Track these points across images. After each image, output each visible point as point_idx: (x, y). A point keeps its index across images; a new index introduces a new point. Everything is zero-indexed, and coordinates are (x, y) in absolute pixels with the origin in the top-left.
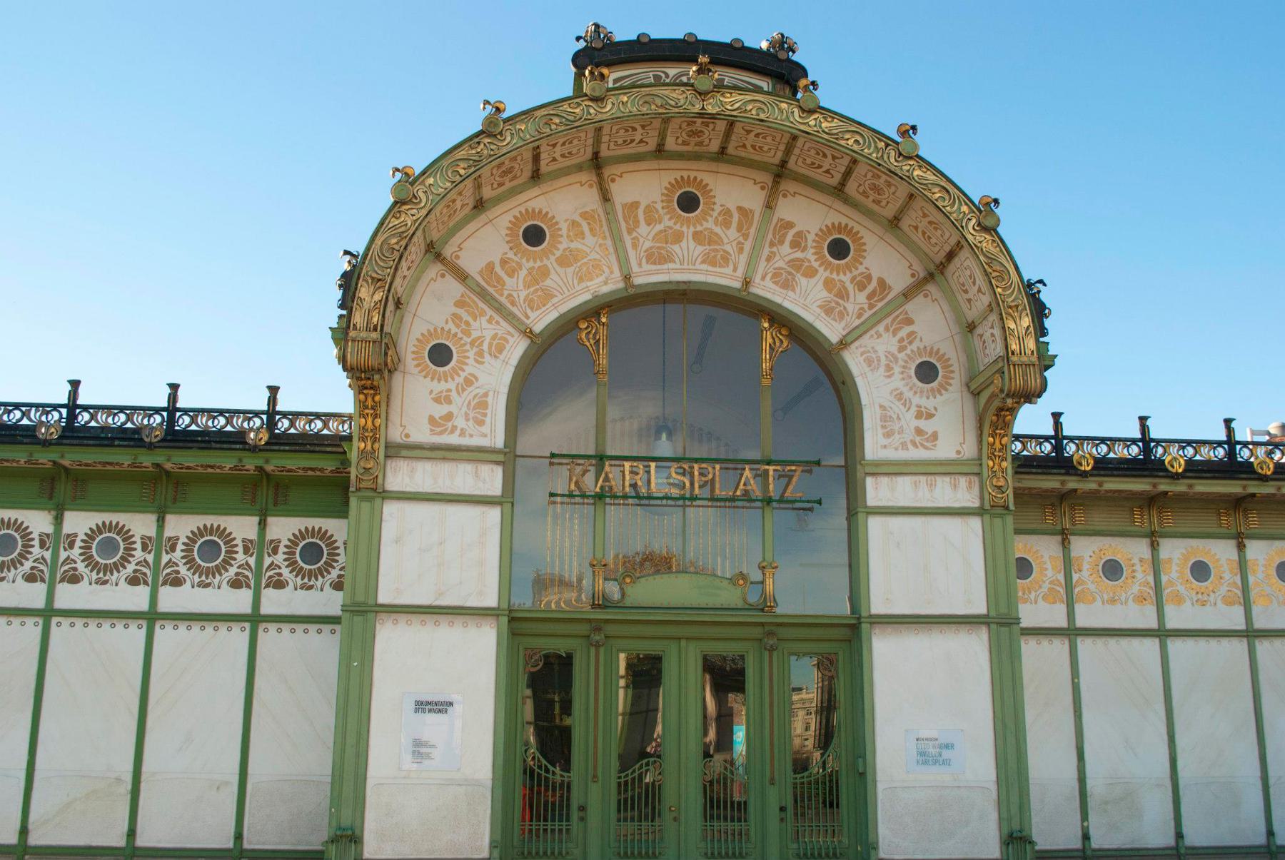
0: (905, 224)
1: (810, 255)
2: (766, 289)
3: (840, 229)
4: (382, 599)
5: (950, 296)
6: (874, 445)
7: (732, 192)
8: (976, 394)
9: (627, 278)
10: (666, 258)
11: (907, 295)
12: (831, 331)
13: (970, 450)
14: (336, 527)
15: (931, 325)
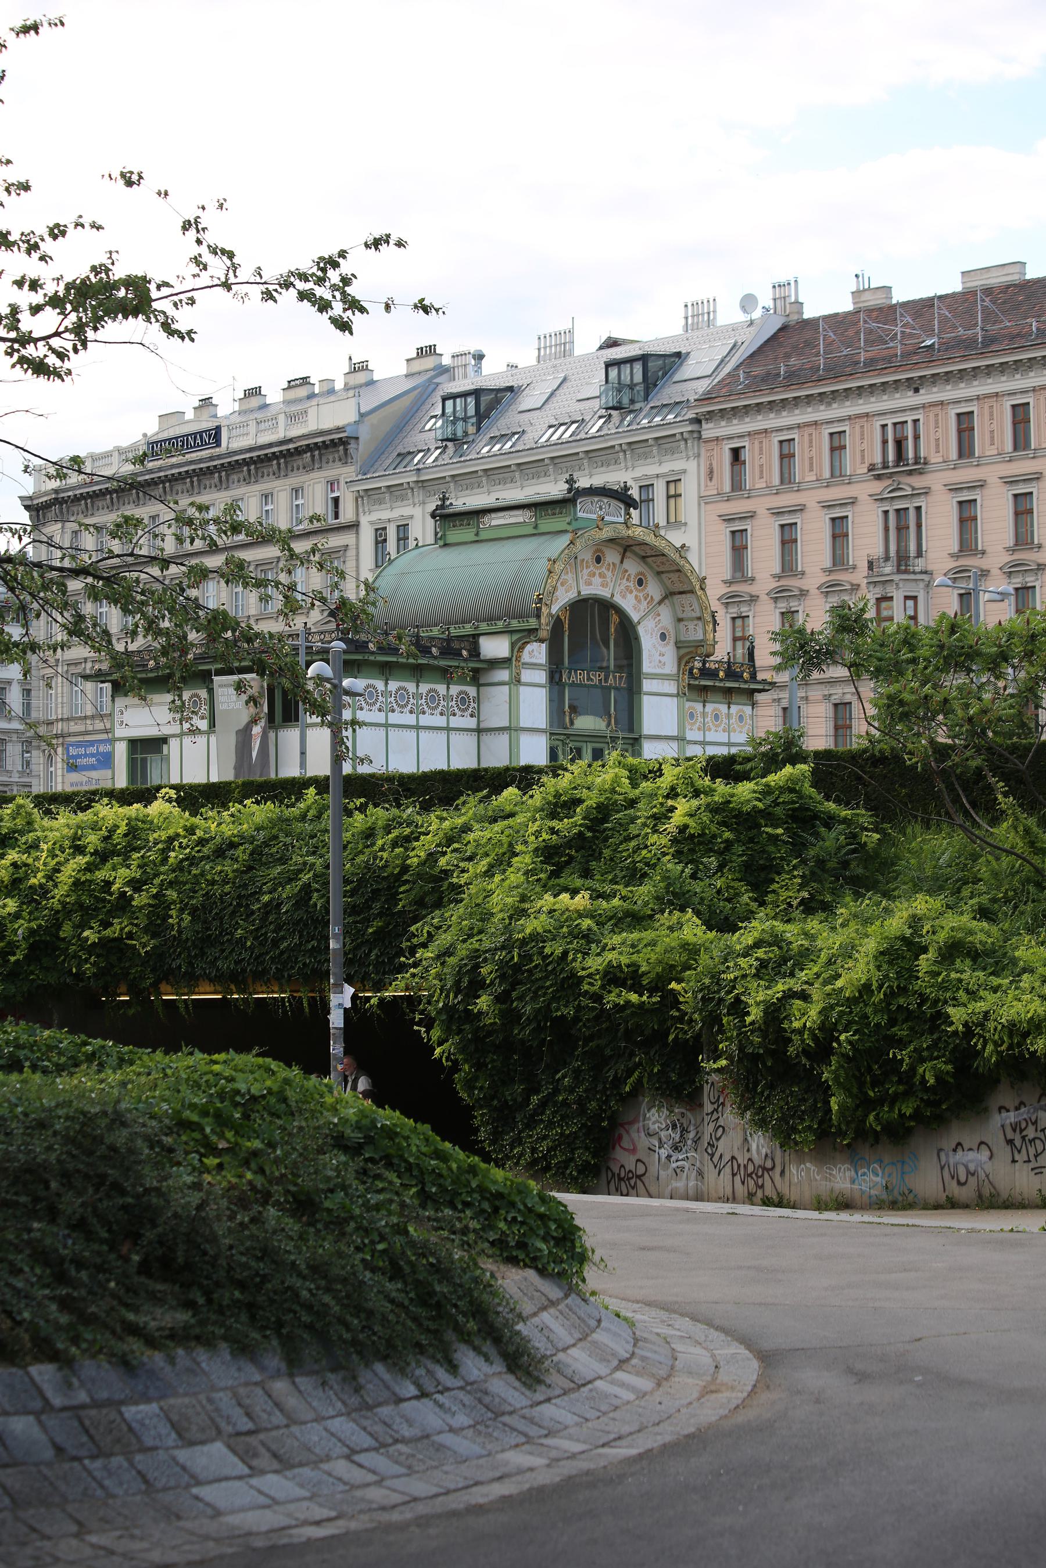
0: (664, 576)
1: (631, 584)
2: (618, 600)
3: (641, 573)
4: (523, 724)
5: (673, 605)
6: (647, 667)
7: (612, 556)
8: (678, 648)
9: (579, 593)
10: (590, 584)
11: (660, 603)
12: (635, 617)
13: (675, 671)
14: (472, 691)
15: (665, 616)
